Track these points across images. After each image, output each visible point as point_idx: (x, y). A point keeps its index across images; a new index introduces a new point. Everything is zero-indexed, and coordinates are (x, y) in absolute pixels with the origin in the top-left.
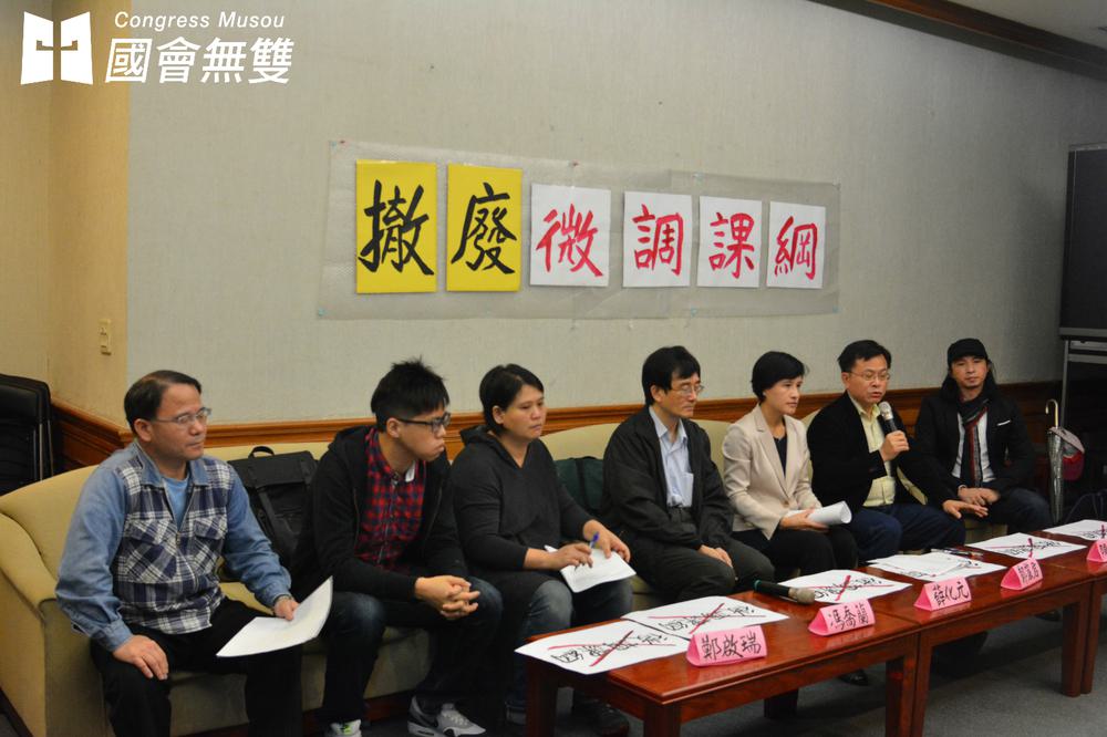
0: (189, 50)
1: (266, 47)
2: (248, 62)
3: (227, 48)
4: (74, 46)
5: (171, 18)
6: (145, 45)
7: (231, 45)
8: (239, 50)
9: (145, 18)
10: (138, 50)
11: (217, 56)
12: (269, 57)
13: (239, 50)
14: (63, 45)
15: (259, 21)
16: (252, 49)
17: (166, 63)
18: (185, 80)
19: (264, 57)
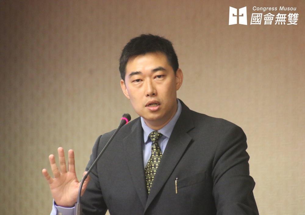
0: (272, 16)
1: (291, 16)
2: (287, 19)
3: (281, 16)
4: (242, 15)
5: (267, 8)
6: (261, 15)
7: (283, 15)
8: (285, 16)
9: (261, 8)
10: (259, 16)
11: (279, 18)
12: (292, 18)
13: (285, 16)
14: (239, 15)
15: (290, 9)
16: (288, 16)
17: (266, 19)
18: (271, 24)
19: (291, 18)
